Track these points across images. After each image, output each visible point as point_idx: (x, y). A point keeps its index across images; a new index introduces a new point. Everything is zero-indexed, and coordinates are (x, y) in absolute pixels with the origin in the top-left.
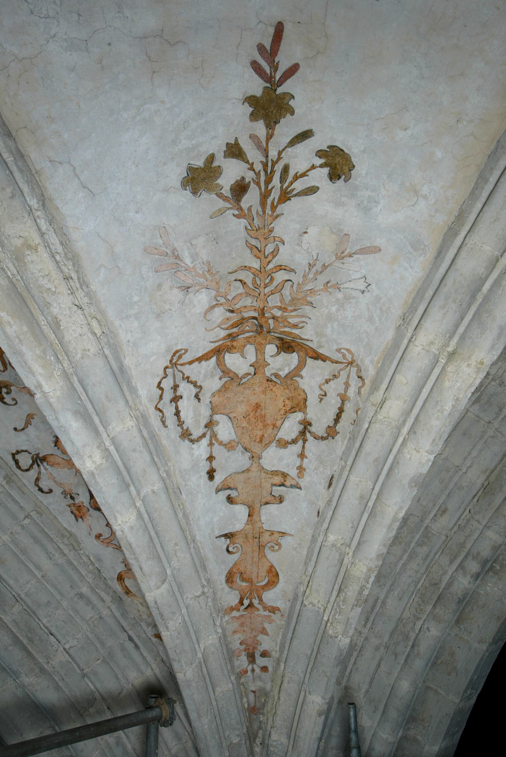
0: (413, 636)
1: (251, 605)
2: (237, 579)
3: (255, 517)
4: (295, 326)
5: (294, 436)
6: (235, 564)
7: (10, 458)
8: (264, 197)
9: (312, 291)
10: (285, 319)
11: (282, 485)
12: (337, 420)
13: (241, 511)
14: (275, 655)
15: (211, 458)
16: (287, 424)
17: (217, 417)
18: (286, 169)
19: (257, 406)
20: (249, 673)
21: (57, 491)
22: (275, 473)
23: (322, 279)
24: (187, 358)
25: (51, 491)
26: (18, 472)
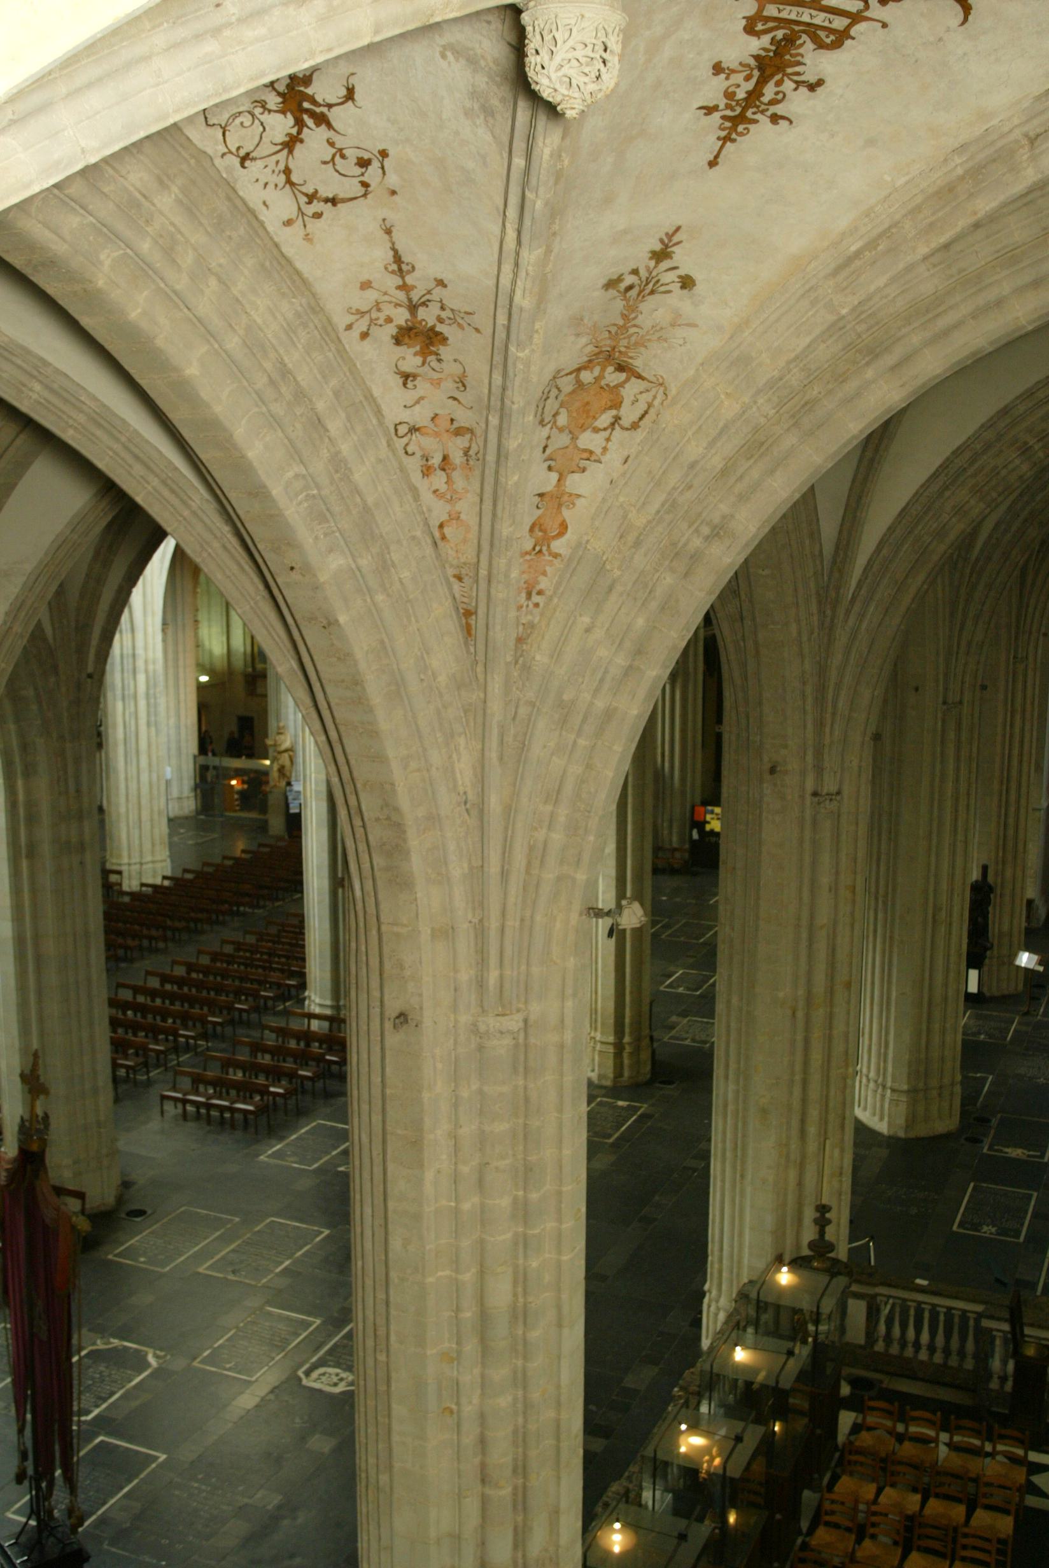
0: (651, 584)
1: (540, 551)
2: (536, 529)
4: (631, 358)
5: (605, 425)
6: (539, 517)
8: (640, 292)
9: (649, 340)
11: (588, 459)
12: (641, 418)
13: (554, 476)
14: (548, 593)
15: (548, 438)
16: (604, 417)
18: (658, 281)
19: (588, 403)
21: (419, 454)
22: (585, 450)
23: (657, 335)
24: (562, 373)
25: (413, 454)
26: (395, 438)
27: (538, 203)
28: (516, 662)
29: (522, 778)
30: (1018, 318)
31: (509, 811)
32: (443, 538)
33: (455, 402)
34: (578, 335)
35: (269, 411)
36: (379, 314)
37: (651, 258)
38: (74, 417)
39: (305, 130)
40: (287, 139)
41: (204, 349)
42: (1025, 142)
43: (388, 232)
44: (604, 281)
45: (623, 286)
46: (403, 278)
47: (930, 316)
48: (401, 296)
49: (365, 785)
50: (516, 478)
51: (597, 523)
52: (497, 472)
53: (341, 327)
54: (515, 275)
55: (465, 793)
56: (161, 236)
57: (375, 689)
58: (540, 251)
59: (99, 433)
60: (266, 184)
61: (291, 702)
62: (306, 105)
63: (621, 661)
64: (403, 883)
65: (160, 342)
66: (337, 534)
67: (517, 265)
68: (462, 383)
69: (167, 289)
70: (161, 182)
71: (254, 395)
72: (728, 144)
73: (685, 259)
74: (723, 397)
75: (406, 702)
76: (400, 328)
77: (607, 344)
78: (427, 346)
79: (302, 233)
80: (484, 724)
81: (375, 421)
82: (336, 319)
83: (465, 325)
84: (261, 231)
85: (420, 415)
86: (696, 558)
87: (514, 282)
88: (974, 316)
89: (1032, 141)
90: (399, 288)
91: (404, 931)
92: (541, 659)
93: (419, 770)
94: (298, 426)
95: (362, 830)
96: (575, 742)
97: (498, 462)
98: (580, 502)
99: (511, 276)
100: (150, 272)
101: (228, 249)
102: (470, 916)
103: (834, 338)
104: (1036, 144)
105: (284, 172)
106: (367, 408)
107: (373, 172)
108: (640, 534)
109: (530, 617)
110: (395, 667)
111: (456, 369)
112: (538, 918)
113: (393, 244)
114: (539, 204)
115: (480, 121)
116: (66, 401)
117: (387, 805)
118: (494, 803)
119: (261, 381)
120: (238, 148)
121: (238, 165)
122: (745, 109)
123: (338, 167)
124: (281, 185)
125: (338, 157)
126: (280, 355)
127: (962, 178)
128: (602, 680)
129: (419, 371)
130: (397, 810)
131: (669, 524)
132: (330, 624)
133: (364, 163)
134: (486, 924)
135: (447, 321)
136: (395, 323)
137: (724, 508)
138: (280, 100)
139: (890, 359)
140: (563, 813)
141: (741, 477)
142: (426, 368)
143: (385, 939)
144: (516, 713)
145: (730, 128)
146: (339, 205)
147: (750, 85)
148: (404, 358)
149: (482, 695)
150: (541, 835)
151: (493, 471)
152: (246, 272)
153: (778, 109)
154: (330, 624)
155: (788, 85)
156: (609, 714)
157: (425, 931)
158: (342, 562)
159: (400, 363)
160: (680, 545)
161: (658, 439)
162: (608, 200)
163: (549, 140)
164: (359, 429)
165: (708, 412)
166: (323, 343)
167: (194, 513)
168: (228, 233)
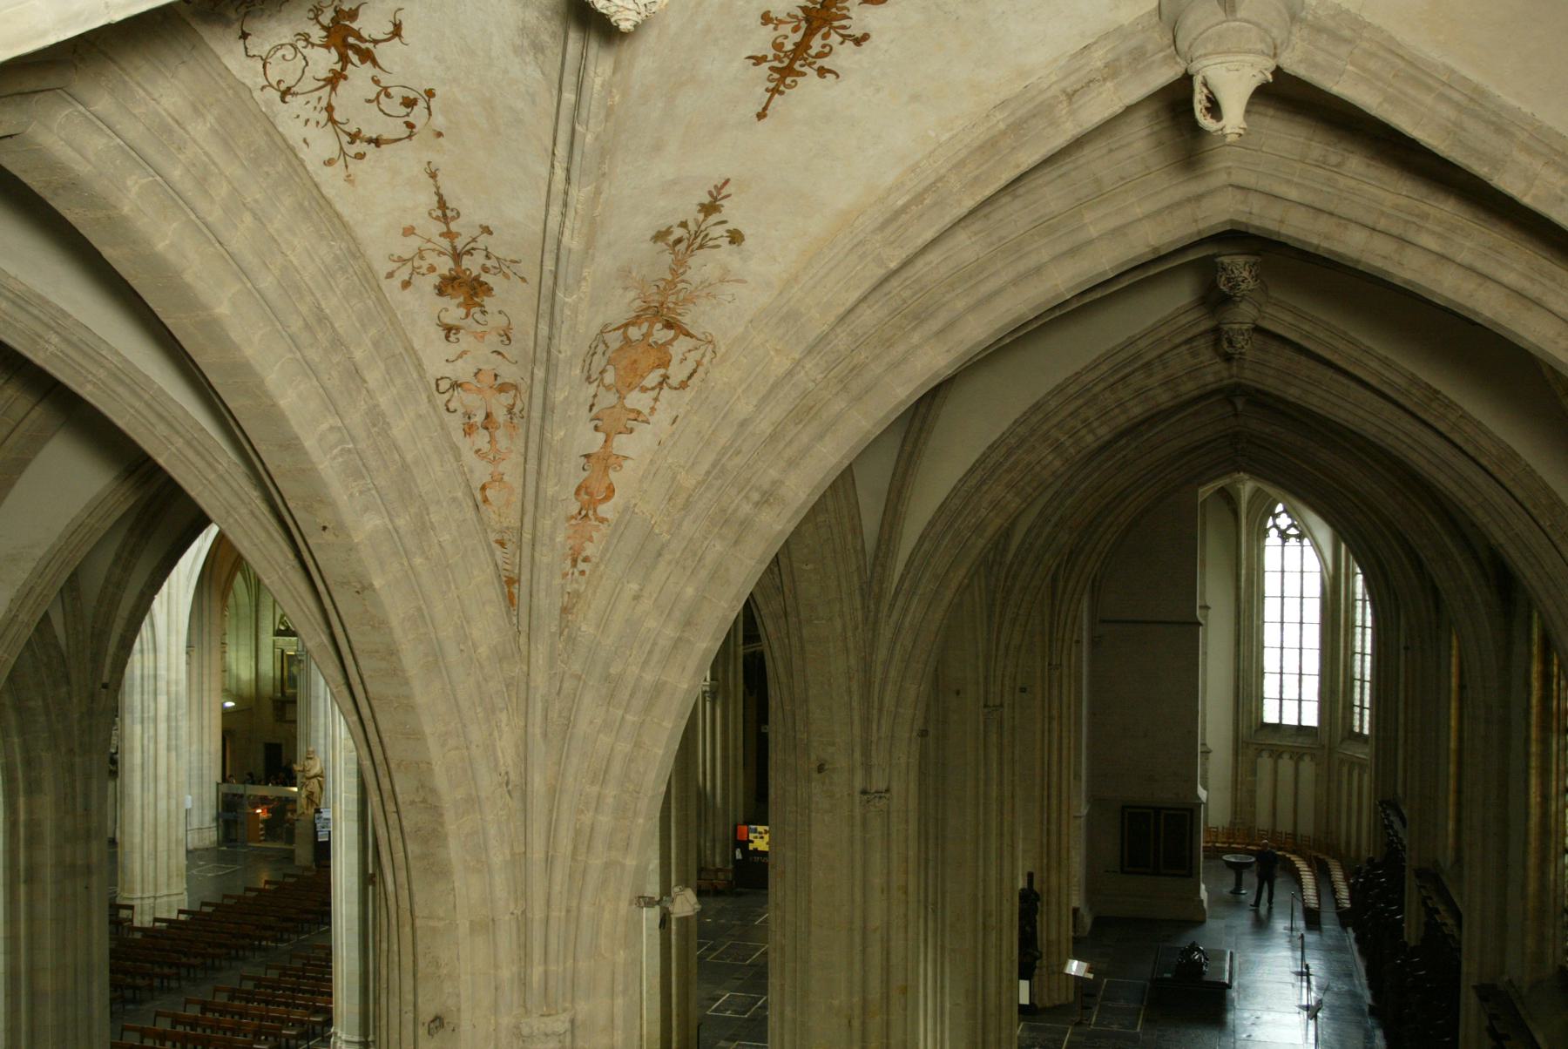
1: (586, 516)
2: (583, 492)
3: (609, 443)
4: (680, 314)
5: (653, 385)
7: (434, 381)
8: (689, 246)
9: (698, 296)
10: (674, 309)
11: (635, 420)
12: (690, 377)
13: (601, 437)
15: (595, 396)
16: (651, 375)
17: (608, 367)
19: (635, 361)
20: (570, 576)
21: (461, 411)
22: (632, 410)
24: (609, 329)
25: (455, 411)
26: (436, 394)
27: (587, 139)
28: (561, 634)
29: (567, 757)
30: (1056, 285)
31: (554, 792)
32: (486, 500)
33: (500, 357)
34: (626, 289)
35: (303, 357)
36: (422, 263)
37: (700, 211)
38: (94, 372)
39: (350, 66)
40: (331, 75)
41: (237, 287)
42: (1063, 98)
43: (433, 175)
44: (653, 233)
45: (672, 238)
46: (447, 224)
47: (973, 282)
48: (445, 243)
49: (399, 765)
50: (562, 433)
51: (645, 486)
52: (542, 428)
53: (382, 274)
54: (564, 215)
55: (507, 773)
56: (194, 165)
57: (411, 660)
58: (590, 188)
59: (120, 390)
60: (307, 121)
61: (322, 682)
62: (351, 40)
63: (670, 632)
64: (441, 872)
65: (188, 277)
66: (374, 492)
67: (565, 205)
68: (507, 336)
69: (198, 221)
70: (196, 110)
71: (289, 341)
72: (776, 96)
73: (734, 213)
74: (772, 353)
75: (444, 673)
76: (443, 277)
77: (655, 299)
78: (471, 297)
79: (343, 174)
80: (527, 699)
81: (415, 375)
82: (376, 266)
83: (511, 274)
84: (300, 169)
85: (463, 370)
86: (745, 525)
87: (562, 225)
88: (1015, 282)
89: (1070, 96)
90: (442, 235)
91: (441, 924)
92: (587, 629)
93: (457, 748)
94: (335, 374)
95: (396, 815)
96: (623, 718)
97: (543, 419)
98: (627, 464)
99: (559, 218)
100: (181, 202)
101: (264, 185)
102: (512, 908)
103: (880, 303)
104: (1073, 100)
105: (326, 109)
106: (407, 359)
107: (419, 112)
108: (690, 496)
109: (575, 586)
110: (433, 636)
111: (502, 321)
112: (586, 908)
113: (438, 188)
114: (589, 138)
115: (529, 58)
116: (85, 354)
117: (423, 786)
118: (538, 783)
119: (296, 325)
120: (279, 82)
121: (279, 99)
122: (793, 61)
123: (381, 106)
124: (322, 123)
125: (382, 96)
126: (317, 300)
127: (1004, 133)
128: (650, 652)
129: (462, 323)
130: (433, 791)
131: (719, 490)
132: (364, 588)
133: (409, 103)
134: (529, 915)
135: (492, 271)
136: (437, 273)
137: (773, 473)
138: (324, 34)
139: (935, 325)
140: (611, 792)
141: (791, 442)
142: (470, 320)
143: (419, 933)
144: (561, 687)
145: (778, 80)
146: (383, 146)
147: (798, 37)
148: (447, 310)
149: (525, 668)
150: (587, 818)
151: (538, 428)
152: (283, 210)
153: (825, 62)
154: (364, 588)
155: (835, 39)
156: (658, 688)
157: (463, 927)
158: (378, 522)
159: (442, 315)
160: (730, 511)
161: (707, 397)
162: (658, 148)
163: (601, 65)
164: (399, 382)
165: (758, 369)
166: (362, 289)
167: (221, 477)
168: (266, 169)
